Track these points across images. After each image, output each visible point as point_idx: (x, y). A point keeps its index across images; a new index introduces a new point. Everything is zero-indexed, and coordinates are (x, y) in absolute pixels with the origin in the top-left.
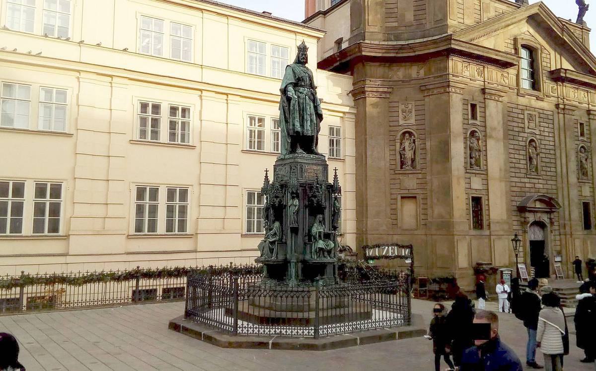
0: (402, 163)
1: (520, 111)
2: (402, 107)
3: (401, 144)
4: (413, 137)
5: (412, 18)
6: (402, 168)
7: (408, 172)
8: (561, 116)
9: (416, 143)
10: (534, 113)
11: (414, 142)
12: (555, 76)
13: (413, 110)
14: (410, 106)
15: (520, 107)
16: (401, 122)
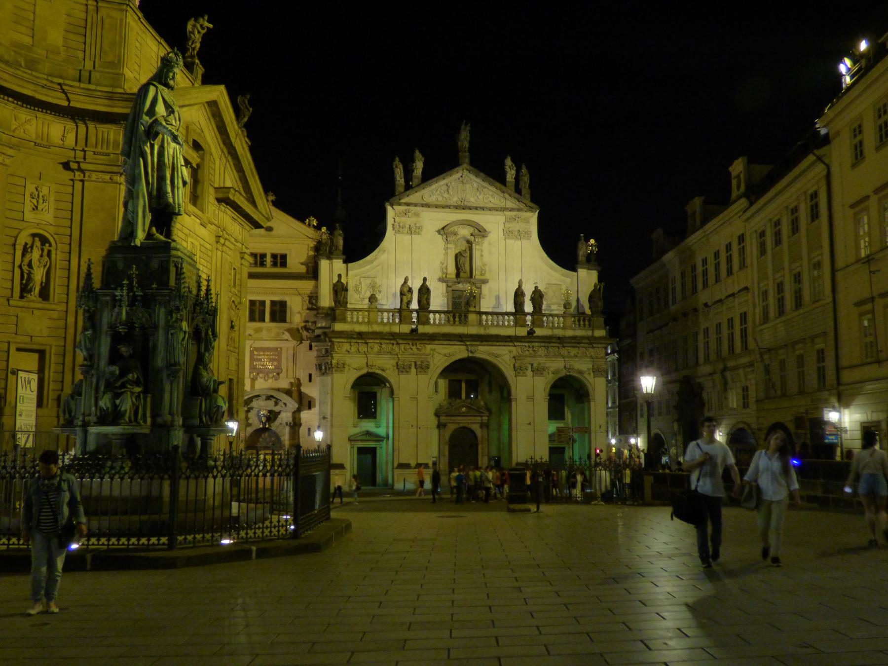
0: (25, 289)
1: (183, 236)
2: (31, 188)
3: (23, 255)
4: (47, 245)
5: (60, 42)
6: (22, 297)
7: (32, 305)
8: (219, 253)
9: (53, 256)
10: (197, 243)
11: (49, 254)
12: (220, 196)
13: (52, 199)
14: (45, 191)
15: (185, 231)
16: (29, 215)
